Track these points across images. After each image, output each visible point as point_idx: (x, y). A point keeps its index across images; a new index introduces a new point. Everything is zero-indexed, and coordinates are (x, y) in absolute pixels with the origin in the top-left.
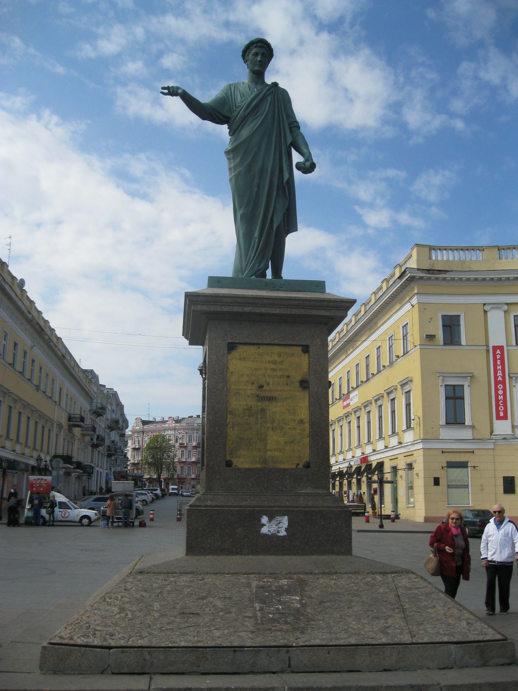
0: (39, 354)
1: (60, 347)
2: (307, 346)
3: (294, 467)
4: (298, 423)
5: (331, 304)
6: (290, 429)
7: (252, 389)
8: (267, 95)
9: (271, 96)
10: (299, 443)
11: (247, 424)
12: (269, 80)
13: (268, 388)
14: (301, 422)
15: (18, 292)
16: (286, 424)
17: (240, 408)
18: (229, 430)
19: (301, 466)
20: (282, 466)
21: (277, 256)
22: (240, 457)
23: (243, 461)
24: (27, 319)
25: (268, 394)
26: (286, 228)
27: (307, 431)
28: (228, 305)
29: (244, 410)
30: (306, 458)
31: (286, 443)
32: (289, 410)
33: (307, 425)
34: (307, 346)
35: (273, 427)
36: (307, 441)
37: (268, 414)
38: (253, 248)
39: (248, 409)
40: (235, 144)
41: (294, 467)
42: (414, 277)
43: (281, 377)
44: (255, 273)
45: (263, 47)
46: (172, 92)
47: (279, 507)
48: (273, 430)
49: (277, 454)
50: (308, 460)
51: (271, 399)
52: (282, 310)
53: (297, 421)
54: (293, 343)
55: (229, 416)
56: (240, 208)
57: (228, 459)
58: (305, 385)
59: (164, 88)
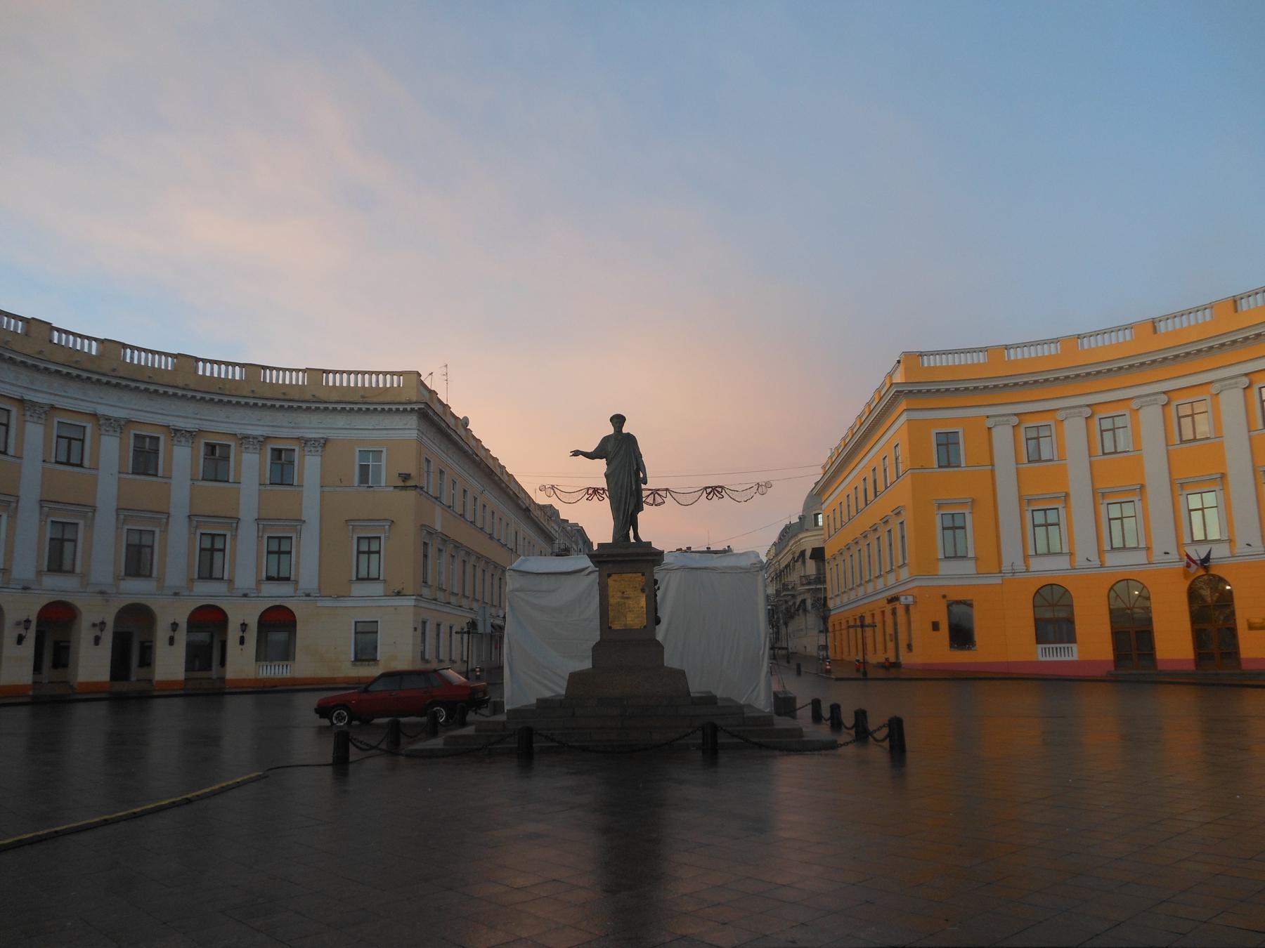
0: (491, 498)
1: (512, 486)
7: (619, 594)
15: (462, 432)
24: (474, 462)
46: (576, 453)
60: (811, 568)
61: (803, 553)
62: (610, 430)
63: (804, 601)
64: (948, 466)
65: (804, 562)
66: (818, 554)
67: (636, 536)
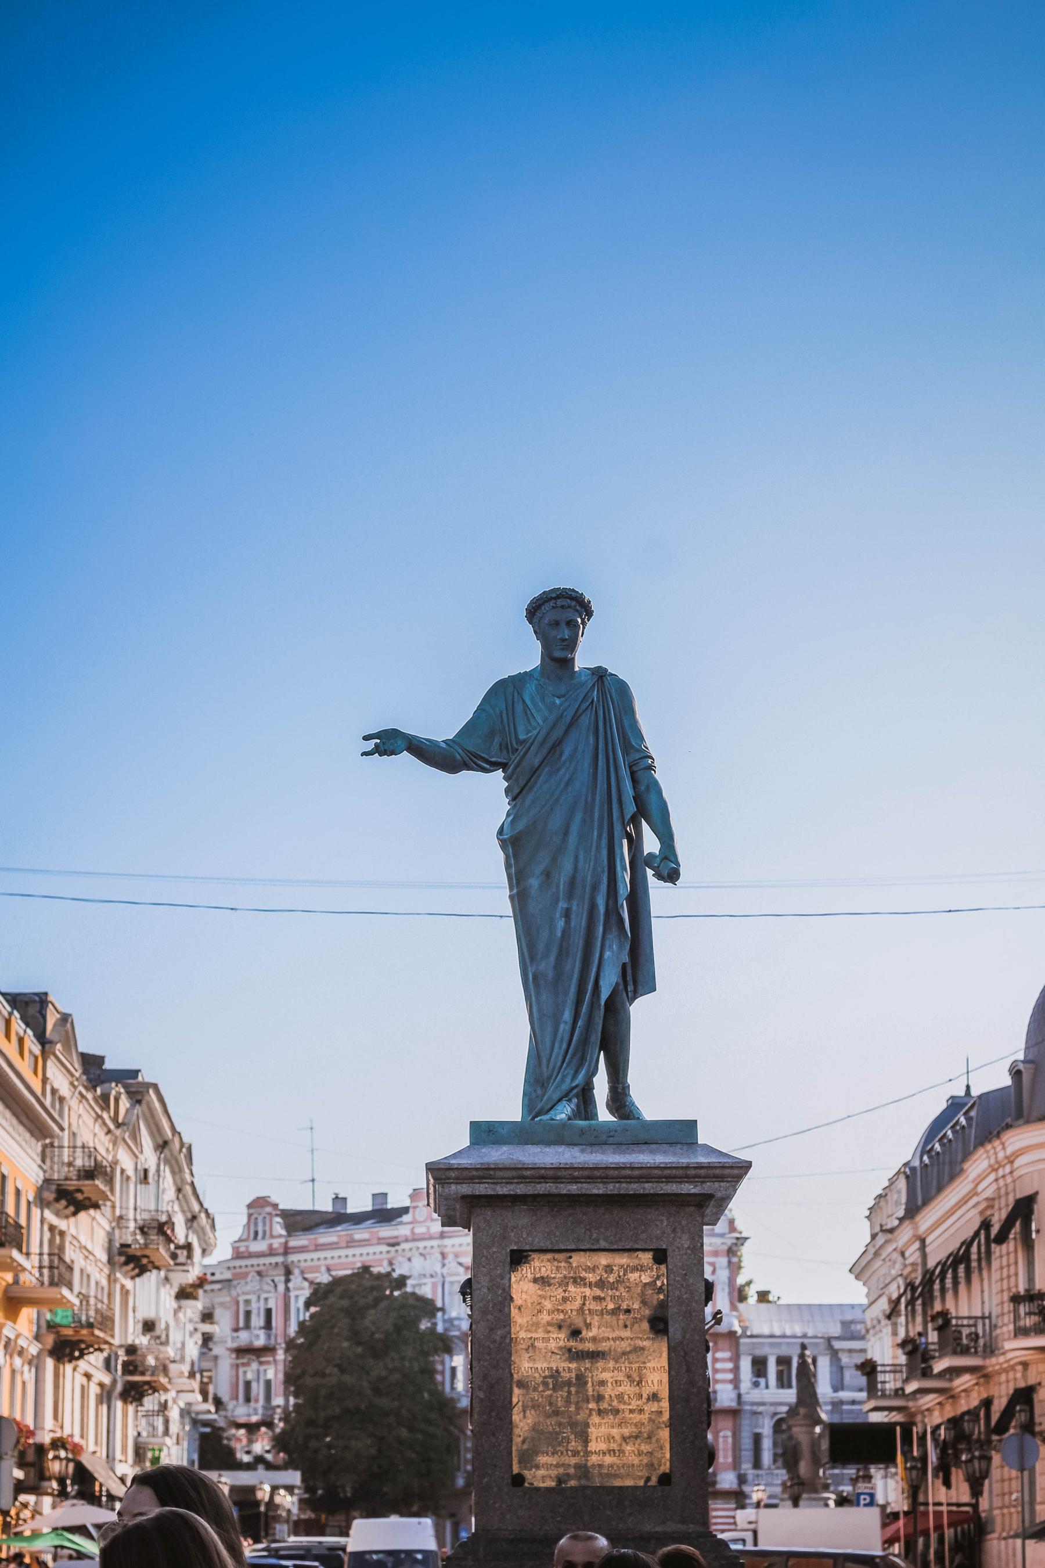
2: (665, 1251)
3: (641, 1483)
4: (648, 1399)
5: (702, 1172)
6: (631, 1411)
7: (559, 1339)
8: (581, 711)
9: (588, 712)
10: (649, 1438)
11: (550, 1404)
12: (583, 660)
13: (590, 1334)
14: (654, 1397)
16: (625, 1403)
17: (537, 1375)
18: (516, 1417)
19: (654, 1481)
20: (617, 1483)
21: (614, 1044)
22: (537, 1467)
25: (590, 1346)
26: (630, 988)
27: (666, 1416)
28: (507, 1183)
29: (545, 1377)
30: (665, 1468)
32: (629, 1377)
33: (665, 1405)
34: (665, 1251)
35: (599, 1410)
36: (665, 1434)
37: (590, 1384)
39: (551, 1377)
40: (521, 826)
41: (641, 1483)
43: (614, 1312)
44: (566, 1095)
45: (569, 607)
48: (599, 1415)
49: (608, 1460)
50: (668, 1471)
51: (595, 1356)
52: (611, 1186)
53: (645, 1396)
54: (636, 1246)
55: (516, 1391)
56: (532, 959)
57: (516, 1469)
58: (661, 1326)
59: (366, 738)
62: (526, 655)
67: (619, 1099)
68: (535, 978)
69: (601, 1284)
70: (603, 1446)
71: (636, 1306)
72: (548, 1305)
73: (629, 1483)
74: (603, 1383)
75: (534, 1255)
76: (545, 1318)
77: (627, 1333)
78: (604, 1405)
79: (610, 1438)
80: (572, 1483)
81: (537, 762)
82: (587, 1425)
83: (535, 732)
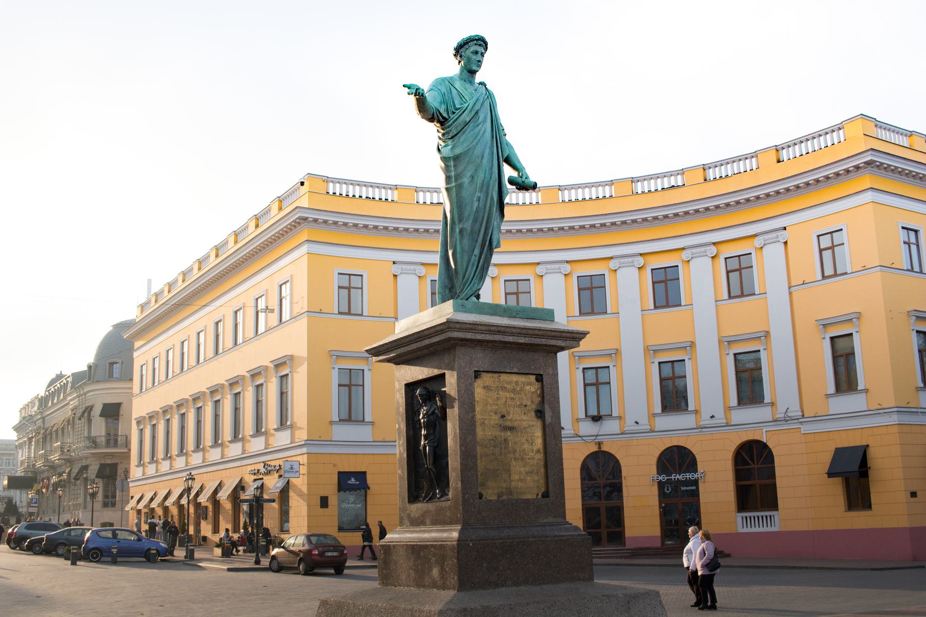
5: (568, 335)
7: (495, 419)
14: (538, 451)
19: (540, 496)
20: (524, 497)
23: (490, 494)
25: (509, 424)
31: (526, 473)
34: (541, 375)
38: (473, 265)
42: (305, 219)
47: (534, 537)
49: (520, 484)
51: (511, 429)
56: (460, 221)
60: (99, 428)
61: (89, 409)
63: (85, 468)
64: (349, 313)
65: (90, 421)
66: (112, 412)
68: (461, 231)
69: (514, 391)
70: (517, 477)
71: (529, 404)
72: (490, 401)
73: (529, 497)
74: (515, 443)
75: (484, 374)
76: (489, 408)
77: (525, 418)
78: (517, 455)
79: (520, 473)
80: (505, 497)
81: (468, 120)
82: (510, 466)
83: (466, 105)
